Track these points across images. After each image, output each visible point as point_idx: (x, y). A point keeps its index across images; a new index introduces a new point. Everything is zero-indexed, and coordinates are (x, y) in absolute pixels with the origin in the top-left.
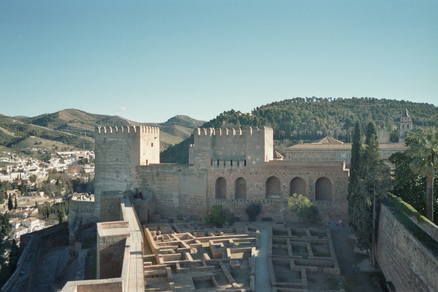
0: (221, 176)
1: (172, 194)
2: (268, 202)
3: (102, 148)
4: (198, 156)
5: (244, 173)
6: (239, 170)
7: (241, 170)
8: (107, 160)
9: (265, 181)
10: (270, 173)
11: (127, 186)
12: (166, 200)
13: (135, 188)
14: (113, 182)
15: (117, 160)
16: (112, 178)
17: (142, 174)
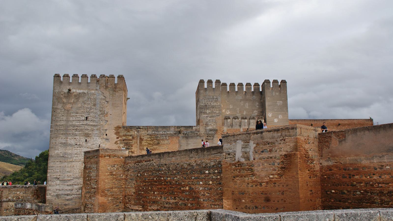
3: (64, 103)
4: (205, 113)
8: (71, 119)
14: (79, 148)
16: (78, 144)
17: (124, 138)
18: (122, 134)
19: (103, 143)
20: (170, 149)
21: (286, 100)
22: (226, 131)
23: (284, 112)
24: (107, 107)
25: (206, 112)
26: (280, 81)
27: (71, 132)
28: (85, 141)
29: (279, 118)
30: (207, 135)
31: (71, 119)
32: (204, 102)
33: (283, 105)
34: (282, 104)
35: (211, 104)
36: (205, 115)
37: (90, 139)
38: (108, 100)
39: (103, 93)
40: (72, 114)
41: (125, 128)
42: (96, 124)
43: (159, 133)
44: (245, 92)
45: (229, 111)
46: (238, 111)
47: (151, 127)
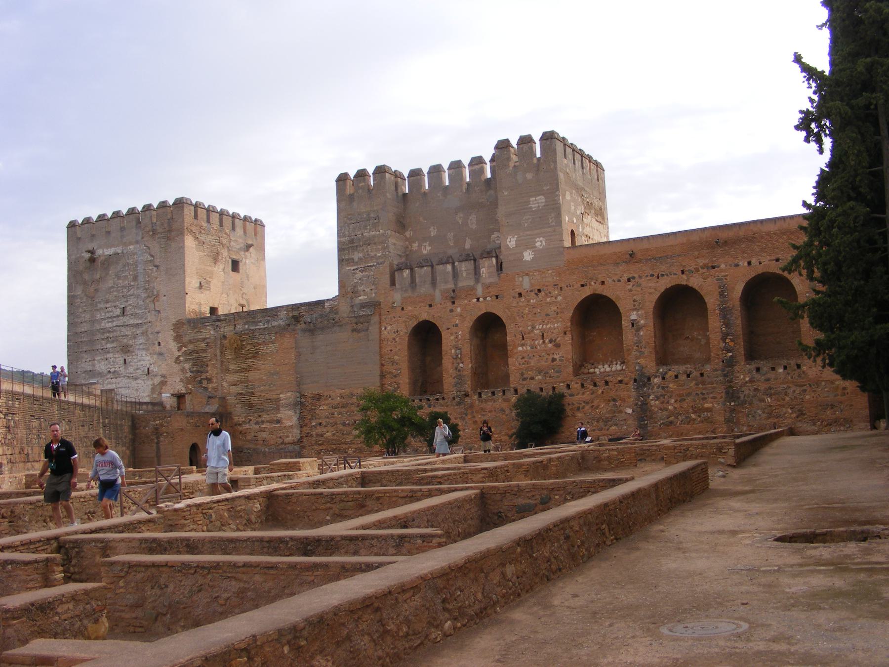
0: (424, 316)
1: (279, 400)
2: (582, 386)
4: (350, 261)
5: (497, 297)
6: (480, 290)
7: (487, 287)
9: (569, 314)
10: (582, 286)
11: (153, 390)
12: (263, 422)
13: (172, 395)
15: (124, 313)
17: (191, 347)
18: (186, 339)
19: (153, 364)
20: (279, 365)
21: (556, 191)
22: (400, 304)
23: (549, 227)
24: (157, 278)
25: (353, 259)
26: (514, 142)
27: (99, 347)
28: (122, 362)
29: (536, 247)
30: (355, 320)
31: (98, 316)
32: (347, 233)
33: (547, 205)
34: (544, 204)
35: (364, 234)
36: (349, 268)
37: (131, 357)
38: (157, 262)
39: (149, 248)
40: (100, 306)
41: (192, 325)
42: (140, 322)
43: (257, 327)
44: (468, 184)
45: (429, 246)
46: (450, 242)
47: (241, 314)
